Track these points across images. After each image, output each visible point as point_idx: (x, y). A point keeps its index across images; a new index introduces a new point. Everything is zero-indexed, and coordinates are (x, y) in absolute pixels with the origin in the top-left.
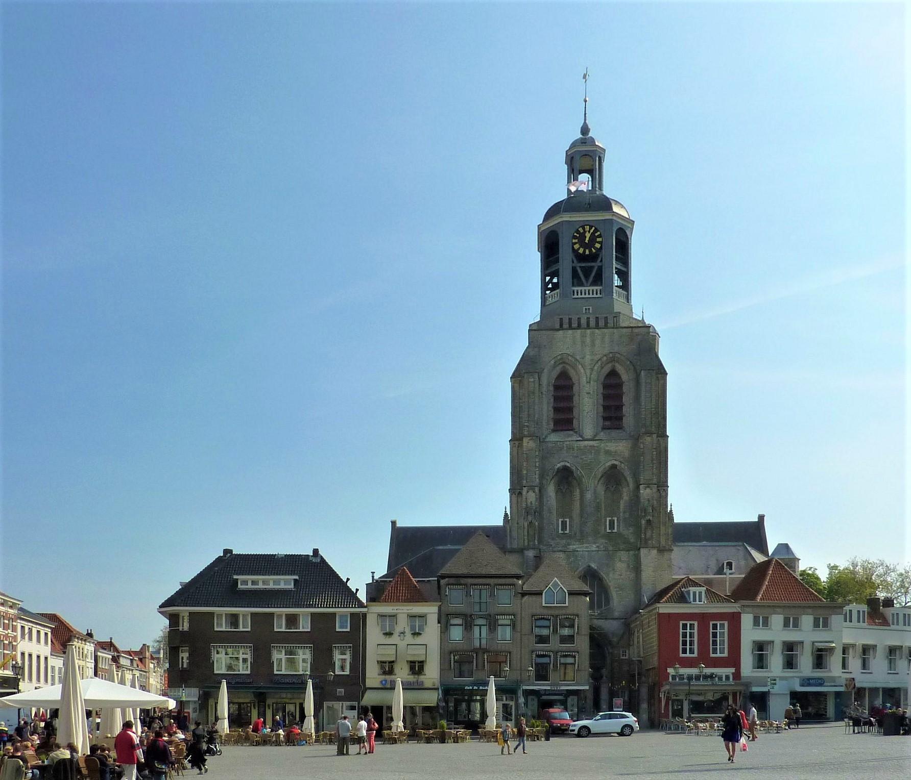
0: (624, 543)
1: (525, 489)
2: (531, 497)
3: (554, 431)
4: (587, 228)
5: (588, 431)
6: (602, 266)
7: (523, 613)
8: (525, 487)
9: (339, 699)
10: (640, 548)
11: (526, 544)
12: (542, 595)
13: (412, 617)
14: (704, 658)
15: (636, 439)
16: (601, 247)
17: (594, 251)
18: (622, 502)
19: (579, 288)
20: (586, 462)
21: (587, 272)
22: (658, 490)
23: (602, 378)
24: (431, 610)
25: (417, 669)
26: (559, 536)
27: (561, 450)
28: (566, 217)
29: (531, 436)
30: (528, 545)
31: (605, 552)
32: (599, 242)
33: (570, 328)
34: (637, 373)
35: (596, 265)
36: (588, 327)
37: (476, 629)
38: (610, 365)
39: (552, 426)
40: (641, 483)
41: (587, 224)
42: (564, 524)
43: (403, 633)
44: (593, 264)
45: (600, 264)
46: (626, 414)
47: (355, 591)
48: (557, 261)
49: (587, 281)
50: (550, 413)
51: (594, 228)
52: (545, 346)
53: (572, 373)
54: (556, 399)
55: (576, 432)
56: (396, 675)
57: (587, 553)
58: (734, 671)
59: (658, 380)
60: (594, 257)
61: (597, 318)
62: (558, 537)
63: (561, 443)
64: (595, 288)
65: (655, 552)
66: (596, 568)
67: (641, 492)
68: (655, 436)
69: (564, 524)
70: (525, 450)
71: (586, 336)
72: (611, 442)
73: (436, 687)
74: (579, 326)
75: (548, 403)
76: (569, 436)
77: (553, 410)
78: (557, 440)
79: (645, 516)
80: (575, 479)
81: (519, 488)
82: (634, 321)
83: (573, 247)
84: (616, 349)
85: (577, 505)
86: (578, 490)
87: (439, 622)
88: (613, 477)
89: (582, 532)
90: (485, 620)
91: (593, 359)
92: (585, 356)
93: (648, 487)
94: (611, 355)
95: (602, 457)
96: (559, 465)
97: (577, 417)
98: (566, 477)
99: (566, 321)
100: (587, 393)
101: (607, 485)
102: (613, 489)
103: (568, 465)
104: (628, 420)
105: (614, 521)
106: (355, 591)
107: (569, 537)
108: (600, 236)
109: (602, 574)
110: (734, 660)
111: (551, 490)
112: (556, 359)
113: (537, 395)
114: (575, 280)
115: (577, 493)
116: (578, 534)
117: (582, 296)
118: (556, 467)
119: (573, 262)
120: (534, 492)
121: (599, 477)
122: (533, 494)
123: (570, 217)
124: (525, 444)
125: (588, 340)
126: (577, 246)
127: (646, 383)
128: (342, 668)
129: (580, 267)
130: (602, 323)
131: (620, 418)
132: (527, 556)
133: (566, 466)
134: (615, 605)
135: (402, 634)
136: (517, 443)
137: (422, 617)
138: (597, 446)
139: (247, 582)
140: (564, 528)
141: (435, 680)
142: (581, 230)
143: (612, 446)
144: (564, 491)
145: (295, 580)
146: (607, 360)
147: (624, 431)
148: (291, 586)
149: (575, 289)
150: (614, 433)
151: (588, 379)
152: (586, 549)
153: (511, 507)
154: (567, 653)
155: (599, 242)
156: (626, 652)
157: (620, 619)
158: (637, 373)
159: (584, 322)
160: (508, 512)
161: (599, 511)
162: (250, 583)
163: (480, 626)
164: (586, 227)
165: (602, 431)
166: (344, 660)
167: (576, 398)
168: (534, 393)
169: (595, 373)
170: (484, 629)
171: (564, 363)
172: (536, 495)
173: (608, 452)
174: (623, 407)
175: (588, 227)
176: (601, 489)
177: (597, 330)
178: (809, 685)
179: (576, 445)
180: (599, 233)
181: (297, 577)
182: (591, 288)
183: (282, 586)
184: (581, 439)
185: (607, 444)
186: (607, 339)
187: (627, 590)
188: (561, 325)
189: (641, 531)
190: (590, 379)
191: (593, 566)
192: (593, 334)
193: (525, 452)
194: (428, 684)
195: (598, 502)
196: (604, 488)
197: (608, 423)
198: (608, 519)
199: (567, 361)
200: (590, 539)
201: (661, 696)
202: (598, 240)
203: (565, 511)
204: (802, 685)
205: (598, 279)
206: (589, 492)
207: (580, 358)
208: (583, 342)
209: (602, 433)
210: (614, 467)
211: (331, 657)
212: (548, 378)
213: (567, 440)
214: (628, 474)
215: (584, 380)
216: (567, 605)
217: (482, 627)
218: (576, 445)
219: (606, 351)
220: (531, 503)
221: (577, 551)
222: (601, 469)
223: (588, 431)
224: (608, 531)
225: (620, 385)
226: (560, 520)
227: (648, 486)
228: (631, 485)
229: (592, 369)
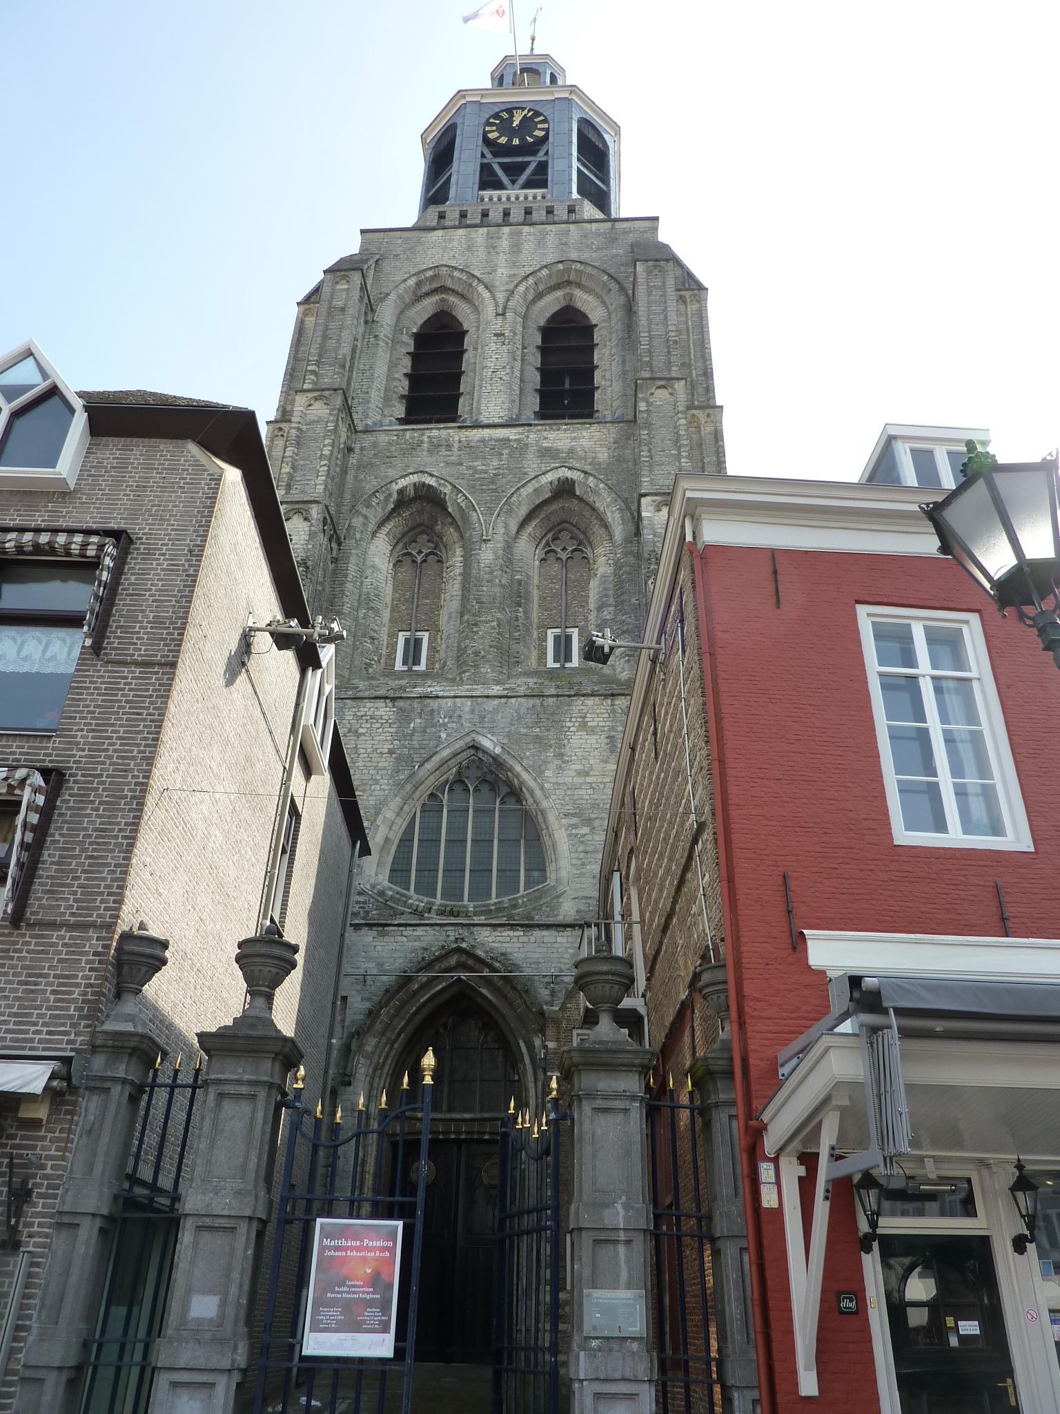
18: (594, 585)
31: (531, 702)
35: (534, 161)
45: (544, 159)
49: (513, 182)
53: (463, 312)
60: (532, 149)
66: (498, 750)
80: (454, 522)
85: (454, 588)
86: (459, 552)
91: (515, 275)
92: (495, 270)
96: (402, 483)
102: (564, 556)
103: (431, 481)
108: (545, 121)
109: (518, 768)
115: (456, 559)
118: (395, 487)
119: (483, 156)
120: (306, 519)
125: (504, 243)
134: (563, 874)
138: (515, 440)
173: (547, 453)
176: (527, 550)
177: (526, 229)
180: (542, 118)
185: (545, 434)
190: (505, 308)
191: (486, 743)
195: (519, 582)
196: (540, 552)
198: (551, 634)
199: (449, 284)
200: (486, 669)
201: (769, 1199)
202: (539, 126)
210: (564, 490)
215: (489, 310)
219: (550, 258)
224: (551, 664)
228: (619, 532)
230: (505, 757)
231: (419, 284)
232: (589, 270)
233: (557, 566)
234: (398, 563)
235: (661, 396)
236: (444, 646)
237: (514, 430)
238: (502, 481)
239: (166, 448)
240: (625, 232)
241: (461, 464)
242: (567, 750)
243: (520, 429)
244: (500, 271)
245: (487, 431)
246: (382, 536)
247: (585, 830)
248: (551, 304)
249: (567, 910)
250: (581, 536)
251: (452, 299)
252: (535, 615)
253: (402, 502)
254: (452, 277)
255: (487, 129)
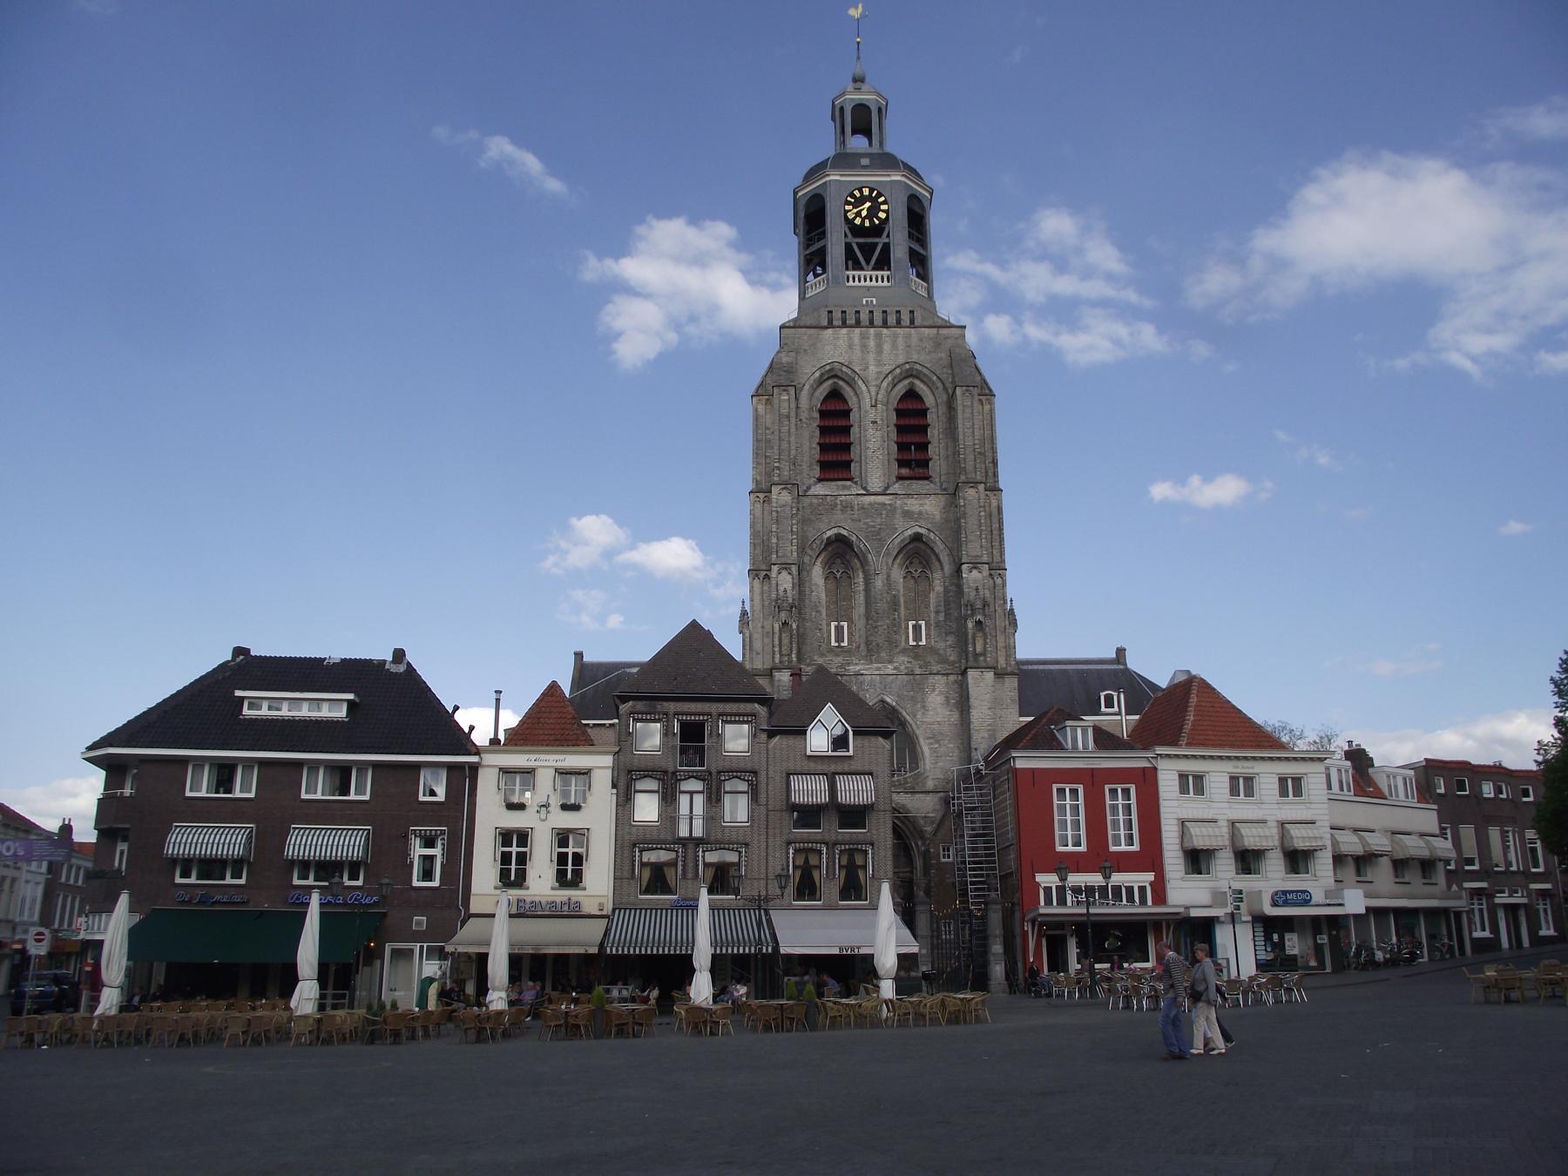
0: (939, 663)
1: (775, 568)
2: (785, 582)
3: (820, 480)
4: (866, 192)
5: (875, 481)
6: (889, 244)
7: (771, 768)
8: (775, 564)
9: (417, 937)
10: (966, 669)
11: (777, 661)
12: (806, 734)
13: (563, 773)
14: (1099, 857)
15: (953, 494)
16: (887, 217)
17: (877, 222)
19: (856, 273)
20: (873, 529)
21: (868, 250)
22: (991, 575)
23: (894, 403)
24: (600, 764)
25: (569, 876)
26: (831, 650)
27: (832, 509)
28: (834, 177)
29: (786, 485)
30: (781, 662)
31: (908, 677)
32: (883, 211)
33: (844, 324)
34: (948, 393)
36: (871, 324)
37: (684, 800)
38: (906, 382)
39: (817, 472)
40: (963, 561)
41: (864, 185)
42: (839, 630)
43: (546, 806)
44: (876, 240)
45: (887, 241)
46: (934, 457)
47: (467, 730)
48: (823, 235)
49: (868, 262)
50: (814, 452)
51: (876, 192)
52: (805, 350)
53: (847, 391)
54: (823, 430)
55: (856, 483)
56: (528, 888)
57: (878, 677)
58: (1153, 879)
59: (982, 404)
60: (877, 231)
61: (885, 312)
62: (828, 652)
63: (833, 498)
64: (880, 273)
65: (990, 675)
66: (894, 704)
67: (964, 575)
68: (981, 487)
69: (839, 630)
70: (774, 505)
71: (868, 338)
72: (912, 498)
73: (604, 913)
74: (858, 324)
75: (811, 437)
76: (848, 488)
77: (819, 449)
78: (827, 493)
79: (972, 615)
81: (764, 568)
82: (939, 321)
83: (846, 218)
84: (915, 357)
86: (861, 575)
87: (614, 786)
88: (917, 552)
89: (868, 643)
90: (702, 783)
91: (880, 372)
92: (868, 368)
93: (975, 568)
94: (907, 366)
95: (899, 522)
96: (829, 533)
97: (857, 459)
98: (841, 552)
99: (837, 315)
100: (874, 422)
101: (907, 568)
102: (916, 575)
103: (845, 533)
104: (938, 466)
105: (920, 626)
106: (467, 730)
107: (847, 652)
108: (885, 202)
109: (904, 713)
110: (1150, 857)
111: (817, 573)
112: (823, 370)
113: (793, 420)
114: (850, 263)
115: (860, 579)
116: (863, 646)
117: (860, 284)
118: (825, 536)
119: (846, 236)
120: (789, 573)
121: (895, 553)
122: (789, 578)
123: (841, 175)
124: (774, 496)
125: (872, 343)
126: (851, 216)
127: (964, 406)
128: (427, 874)
129: (857, 243)
130: (892, 319)
131: (925, 463)
132: (779, 681)
133: (840, 534)
134: (928, 767)
135: (543, 809)
136: (761, 496)
137: (585, 773)
138: (890, 504)
139: (262, 705)
140: (839, 638)
141: (603, 900)
142: (857, 193)
143: (913, 505)
144: (838, 577)
145: (350, 703)
146: (901, 373)
147: (931, 482)
148: (341, 713)
149: (851, 273)
150: (917, 486)
151: (873, 401)
152: (877, 672)
153: (752, 600)
154: (851, 846)
155: (883, 211)
156: (949, 851)
157: (937, 792)
158: (948, 393)
159: (864, 317)
160: (748, 608)
161: (895, 610)
162: (265, 705)
163: (691, 793)
164: (864, 189)
165: (897, 482)
166: (428, 860)
167: (854, 431)
168: (788, 417)
169: (882, 392)
170: (699, 800)
171: (836, 376)
172: (793, 578)
173: (908, 514)
174: (929, 446)
175: (867, 190)
176: (897, 574)
178: (1286, 903)
179: (856, 500)
180: (882, 199)
181: (351, 696)
182: (874, 273)
183: (325, 712)
184: (864, 492)
185: (905, 501)
186: (900, 341)
187: (946, 742)
188: (830, 321)
189: (966, 640)
190: (876, 400)
191: (889, 700)
192: (878, 336)
193: (775, 509)
194: (590, 907)
195: (895, 596)
196: (903, 573)
197: (905, 471)
198: (911, 623)
199: (839, 374)
200: (883, 654)
201: (1026, 928)
202: (884, 207)
203: (840, 609)
204: (1275, 904)
205: (884, 263)
206: (880, 577)
207: (861, 370)
208: (864, 347)
209: (897, 486)
210: (917, 538)
211: (406, 852)
212: (810, 401)
213: (841, 493)
214: (940, 547)
215: (867, 402)
216: (851, 753)
217: (695, 796)
218: (856, 500)
219: (901, 360)
220: (785, 591)
221: (862, 675)
222: (897, 541)
223: (875, 481)
224: (912, 643)
225: (923, 413)
226: (833, 624)
227: (975, 566)
228: (948, 568)
229: (879, 387)
230: (898, 707)
231: (822, 375)
232: (925, 370)
233: (912, 582)
234: (826, 579)
235: (971, 492)
236: (858, 635)
237: (888, 497)
238: (883, 534)
239: (873, 739)
240: (947, 338)
241: (860, 521)
242: (927, 704)
243: (891, 497)
244: (872, 368)
245: (873, 497)
246: (818, 563)
247: (937, 746)
248: (902, 388)
249: (930, 784)
250: (924, 563)
251: (841, 383)
252: (903, 617)
253: (830, 542)
254: (842, 371)
255: (847, 208)
